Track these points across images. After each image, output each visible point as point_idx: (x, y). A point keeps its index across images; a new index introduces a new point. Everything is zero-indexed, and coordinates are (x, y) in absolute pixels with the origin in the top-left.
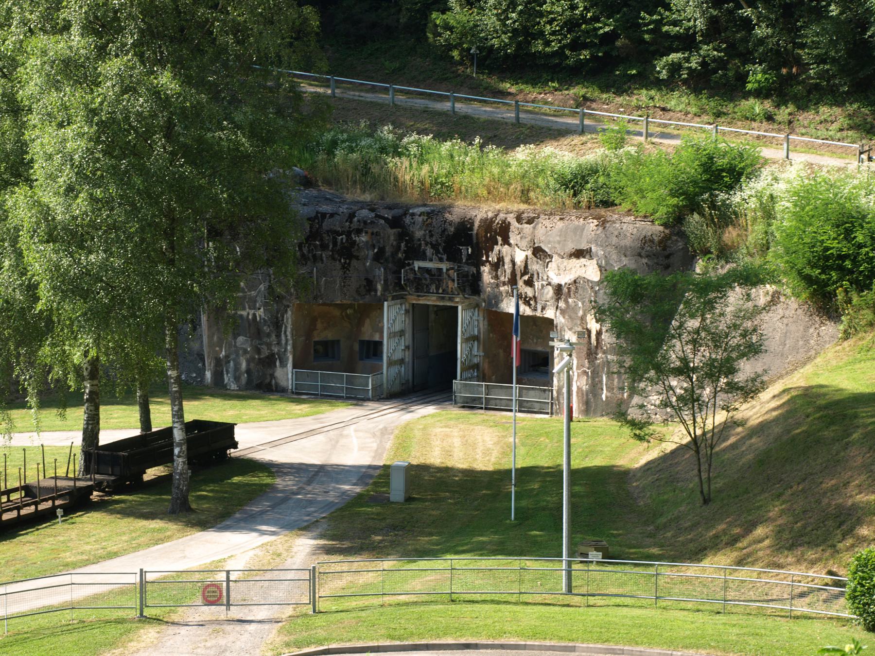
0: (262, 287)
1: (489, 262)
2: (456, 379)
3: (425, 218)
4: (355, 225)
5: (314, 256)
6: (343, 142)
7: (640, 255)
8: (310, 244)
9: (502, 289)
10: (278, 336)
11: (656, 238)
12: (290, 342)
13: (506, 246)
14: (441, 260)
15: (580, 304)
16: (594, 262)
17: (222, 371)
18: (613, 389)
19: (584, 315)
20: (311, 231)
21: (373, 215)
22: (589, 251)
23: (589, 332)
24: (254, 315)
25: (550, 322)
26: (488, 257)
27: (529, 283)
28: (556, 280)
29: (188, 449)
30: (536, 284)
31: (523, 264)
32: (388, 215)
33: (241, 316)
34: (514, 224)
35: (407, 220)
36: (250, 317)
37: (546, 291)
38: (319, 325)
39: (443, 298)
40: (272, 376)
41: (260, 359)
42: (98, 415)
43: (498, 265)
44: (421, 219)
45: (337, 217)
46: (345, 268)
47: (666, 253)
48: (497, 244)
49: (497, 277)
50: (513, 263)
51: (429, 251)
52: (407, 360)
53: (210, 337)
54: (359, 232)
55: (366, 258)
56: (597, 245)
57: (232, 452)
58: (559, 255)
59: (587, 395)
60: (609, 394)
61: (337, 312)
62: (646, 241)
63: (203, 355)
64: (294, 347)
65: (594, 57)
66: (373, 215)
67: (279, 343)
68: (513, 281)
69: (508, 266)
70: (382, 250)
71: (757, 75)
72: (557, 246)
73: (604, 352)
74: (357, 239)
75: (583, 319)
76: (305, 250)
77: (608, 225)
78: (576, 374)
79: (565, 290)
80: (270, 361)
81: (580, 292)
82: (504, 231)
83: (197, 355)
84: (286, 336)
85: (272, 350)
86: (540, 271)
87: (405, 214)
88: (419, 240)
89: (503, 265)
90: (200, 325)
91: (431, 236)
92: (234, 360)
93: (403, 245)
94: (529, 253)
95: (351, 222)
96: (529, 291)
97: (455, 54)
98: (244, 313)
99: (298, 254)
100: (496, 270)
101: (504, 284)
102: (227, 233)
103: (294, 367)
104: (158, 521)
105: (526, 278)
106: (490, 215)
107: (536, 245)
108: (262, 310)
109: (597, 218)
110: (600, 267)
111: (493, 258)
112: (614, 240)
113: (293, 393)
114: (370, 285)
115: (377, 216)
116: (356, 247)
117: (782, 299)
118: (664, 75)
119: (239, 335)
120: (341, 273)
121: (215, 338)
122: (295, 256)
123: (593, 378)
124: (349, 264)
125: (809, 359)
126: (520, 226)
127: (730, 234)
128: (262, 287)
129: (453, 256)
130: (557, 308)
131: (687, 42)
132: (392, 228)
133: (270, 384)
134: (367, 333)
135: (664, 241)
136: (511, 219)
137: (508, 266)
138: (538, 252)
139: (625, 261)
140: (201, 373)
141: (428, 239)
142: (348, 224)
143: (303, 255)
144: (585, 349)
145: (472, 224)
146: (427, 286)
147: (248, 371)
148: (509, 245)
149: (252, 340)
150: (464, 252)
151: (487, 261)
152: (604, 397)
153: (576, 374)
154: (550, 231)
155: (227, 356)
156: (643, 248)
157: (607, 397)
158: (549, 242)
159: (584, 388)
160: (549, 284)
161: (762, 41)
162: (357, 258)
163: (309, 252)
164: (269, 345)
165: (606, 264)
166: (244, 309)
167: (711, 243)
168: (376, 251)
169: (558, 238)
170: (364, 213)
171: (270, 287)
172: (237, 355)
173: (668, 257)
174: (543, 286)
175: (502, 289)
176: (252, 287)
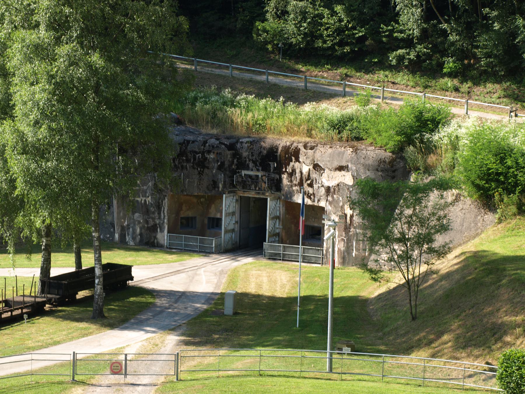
0: (150, 184)
1: (287, 172)
2: (265, 241)
3: (249, 145)
4: (207, 148)
5: (182, 166)
6: (201, 98)
7: (377, 170)
8: (180, 159)
9: (294, 188)
10: (159, 214)
11: (387, 160)
12: (166, 217)
13: (297, 163)
14: (258, 170)
15: (341, 199)
16: (350, 173)
17: (125, 234)
18: (359, 250)
19: (343, 205)
20: (180, 151)
21: (218, 142)
22: (347, 167)
23: (346, 215)
24: (145, 201)
25: (323, 209)
26: (286, 169)
27: (311, 185)
28: (326, 184)
29: (104, 280)
30: (315, 186)
31: (307, 174)
32: (227, 142)
33: (137, 201)
34: (302, 150)
35: (238, 146)
36: (143, 202)
37: (320, 190)
38: (184, 208)
39: (259, 193)
40: (155, 237)
41: (148, 227)
42: (50, 258)
43: (292, 174)
44: (246, 145)
45: (197, 143)
46: (200, 173)
47: (393, 169)
48: (292, 161)
49: (291, 181)
50: (301, 173)
51: (251, 165)
52: (236, 229)
53: (119, 213)
54: (209, 152)
55: (213, 168)
56: (352, 163)
57: (130, 283)
58: (329, 169)
59: (344, 253)
60: (357, 253)
61: (195, 200)
62: (381, 161)
63: (114, 224)
64: (168, 220)
65: (352, 51)
66: (218, 142)
67: (160, 218)
68: (301, 184)
69: (298, 175)
70: (223, 164)
71: (450, 64)
72: (328, 163)
73: (355, 228)
74: (208, 156)
75: (342, 207)
76: (177, 163)
77: (358, 152)
78: (337, 240)
79: (332, 190)
80: (154, 229)
81: (341, 191)
82: (296, 154)
83: (111, 224)
84: (164, 214)
85: (155, 222)
86: (317, 178)
87: (237, 142)
88: (245, 158)
89: (295, 174)
90: (113, 206)
91: (253, 156)
92: (132, 227)
93: (235, 161)
94: (311, 167)
95: (205, 146)
96: (310, 190)
97: (269, 47)
98: (139, 199)
99: (173, 164)
100: (291, 177)
101: (296, 185)
102: (130, 151)
103: (168, 232)
104: (85, 323)
105: (309, 182)
106: (288, 144)
107: (315, 163)
108: (150, 197)
109: (352, 147)
110: (353, 176)
111: (289, 169)
112: (362, 161)
113: (167, 248)
114: (215, 184)
115: (221, 143)
116: (207, 161)
117: (462, 198)
118: (394, 62)
119: (136, 212)
120: (198, 176)
121: (121, 214)
122: (170, 166)
123: (348, 243)
124: (203, 172)
125: (477, 235)
126: (306, 151)
127: (432, 159)
128: (150, 184)
129: (265, 168)
130: (327, 200)
131: (408, 43)
132: (229, 150)
133: (154, 242)
134: (213, 213)
135: (392, 162)
136: (301, 146)
137: (298, 175)
138: (316, 167)
139: (368, 173)
140: (113, 234)
141: (250, 157)
142: (202, 147)
143: (175, 165)
144: (343, 225)
145: (277, 149)
146: (249, 186)
147: (141, 234)
148: (299, 162)
149: (143, 216)
150: (272, 166)
151: (286, 171)
152: (354, 254)
153: (337, 240)
154: (324, 154)
155: (128, 225)
156: (379, 166)
157: (355, 255)
158: (323, 161)
159: (342, 249)
160: (323, 186)
161: (453, 44)
162: (208, 168)
163: (179, 163)
164: (153, 219)
165: (357, 175)
166: (139, 197)
167: (420, 164)
168: (219, 164)
169: (328, 159)
170: (213, 141)
171: (155, 184)
172: (135, 224)
173: (394, 171)
174: (319, 187)
175: (294, 188)
176: (144, 183)
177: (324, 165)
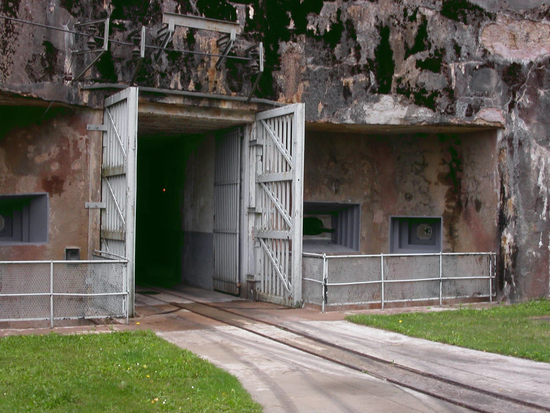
27: (434, 64)
30: (452, 66)
96: (431, 81)
101: (354, 71)
105: (422, 56)
130: (511, 106)
146: (163, 75)
160: (490, 65)
174: (471, 70)
177: (492, 6)
